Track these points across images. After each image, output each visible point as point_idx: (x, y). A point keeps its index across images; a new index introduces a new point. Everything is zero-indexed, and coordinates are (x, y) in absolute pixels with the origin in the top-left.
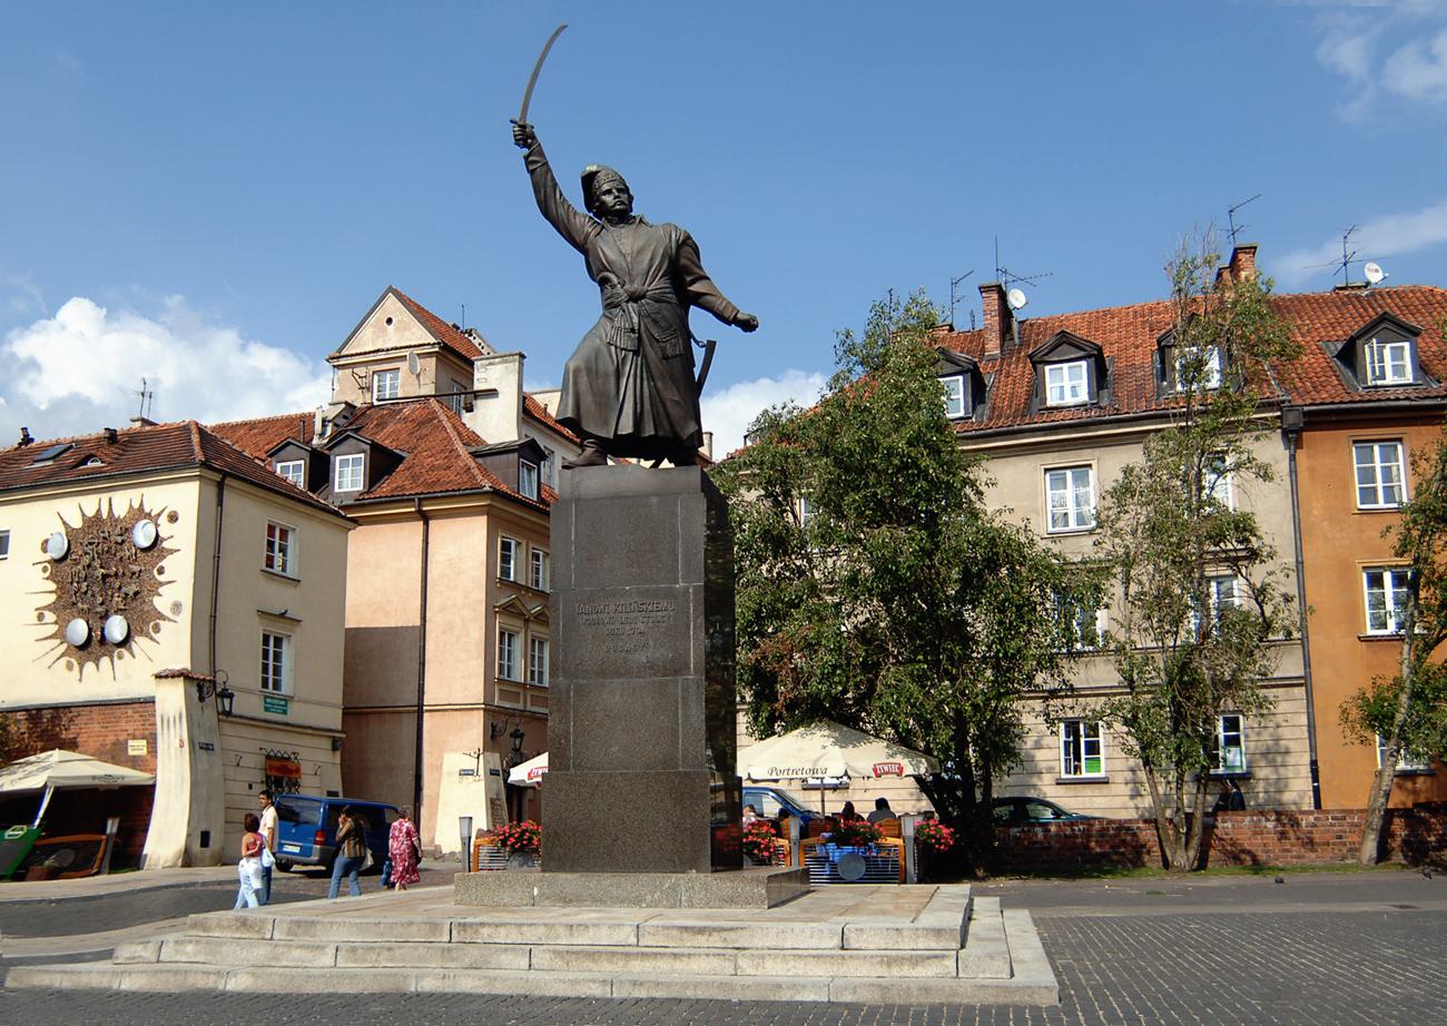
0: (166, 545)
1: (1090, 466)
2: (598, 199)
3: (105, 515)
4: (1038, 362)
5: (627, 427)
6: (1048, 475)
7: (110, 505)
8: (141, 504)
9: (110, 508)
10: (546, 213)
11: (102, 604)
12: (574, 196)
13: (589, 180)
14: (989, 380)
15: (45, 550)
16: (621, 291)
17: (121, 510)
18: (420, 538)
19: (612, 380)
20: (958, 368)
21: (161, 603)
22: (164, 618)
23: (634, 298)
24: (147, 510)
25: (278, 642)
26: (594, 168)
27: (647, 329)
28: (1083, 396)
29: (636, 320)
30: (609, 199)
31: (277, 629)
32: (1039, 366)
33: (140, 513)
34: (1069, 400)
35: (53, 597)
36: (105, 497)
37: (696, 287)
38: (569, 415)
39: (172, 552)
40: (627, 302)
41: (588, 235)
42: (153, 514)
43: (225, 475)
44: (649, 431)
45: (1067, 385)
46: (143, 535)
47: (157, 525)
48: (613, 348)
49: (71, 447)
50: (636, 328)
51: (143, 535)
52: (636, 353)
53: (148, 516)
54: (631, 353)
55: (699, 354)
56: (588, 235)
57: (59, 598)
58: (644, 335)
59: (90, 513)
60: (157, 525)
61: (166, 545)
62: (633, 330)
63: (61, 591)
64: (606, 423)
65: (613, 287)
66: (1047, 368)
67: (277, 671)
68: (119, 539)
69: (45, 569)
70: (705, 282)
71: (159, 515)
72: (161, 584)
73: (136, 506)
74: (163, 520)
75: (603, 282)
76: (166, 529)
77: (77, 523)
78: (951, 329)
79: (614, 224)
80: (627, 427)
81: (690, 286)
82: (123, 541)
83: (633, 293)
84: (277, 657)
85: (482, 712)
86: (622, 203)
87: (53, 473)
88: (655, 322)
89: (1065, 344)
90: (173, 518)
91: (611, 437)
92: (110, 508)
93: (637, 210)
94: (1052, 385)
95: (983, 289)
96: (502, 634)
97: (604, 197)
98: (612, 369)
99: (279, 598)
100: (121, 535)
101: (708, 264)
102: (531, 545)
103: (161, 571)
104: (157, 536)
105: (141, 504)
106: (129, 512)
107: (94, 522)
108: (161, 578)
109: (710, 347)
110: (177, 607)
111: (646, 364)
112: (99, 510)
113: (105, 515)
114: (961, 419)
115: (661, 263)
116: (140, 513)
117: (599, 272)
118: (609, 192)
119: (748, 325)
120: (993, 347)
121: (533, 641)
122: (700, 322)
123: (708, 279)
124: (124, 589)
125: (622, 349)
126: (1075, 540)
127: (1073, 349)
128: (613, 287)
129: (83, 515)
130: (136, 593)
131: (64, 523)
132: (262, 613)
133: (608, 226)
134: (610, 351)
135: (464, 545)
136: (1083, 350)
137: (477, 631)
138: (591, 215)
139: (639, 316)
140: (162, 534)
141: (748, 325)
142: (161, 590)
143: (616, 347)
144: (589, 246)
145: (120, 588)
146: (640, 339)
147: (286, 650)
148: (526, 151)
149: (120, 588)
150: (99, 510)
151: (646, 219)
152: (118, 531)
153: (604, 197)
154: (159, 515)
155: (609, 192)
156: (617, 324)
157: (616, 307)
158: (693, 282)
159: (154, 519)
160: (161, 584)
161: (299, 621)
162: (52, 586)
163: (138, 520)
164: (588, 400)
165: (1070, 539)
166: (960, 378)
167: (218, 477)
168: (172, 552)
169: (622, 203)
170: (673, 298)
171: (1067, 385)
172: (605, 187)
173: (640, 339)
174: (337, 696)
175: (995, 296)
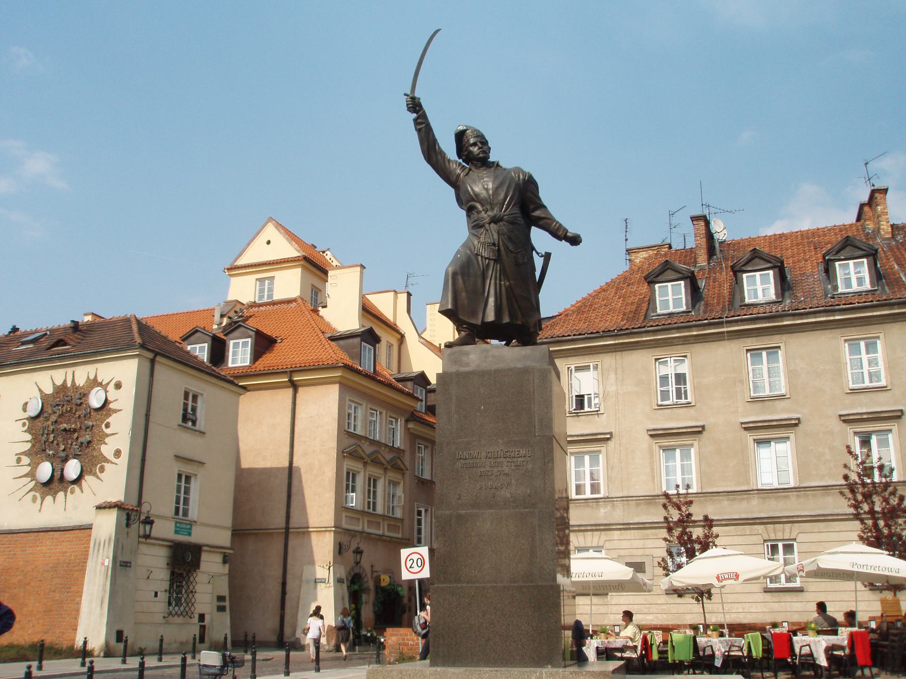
0: (111, 406)
1: (779, 347)
2: (467, 149)
3: (69, 384)
4: (737, 271)
5: (491, 317)
6: (749, 354)
8: (96, 376)
9: (73, 379)
11: (64, 450)
12: (448, 147)
13: (460, 137)
14: (702, 284)
15: (25, 410)
17: (81, 381)
18: (290, 401)
19: (480, 282)
20: (680, 275)
21: (107, 450)
22: (107, 461)
23: (495, 220)
24: (100, 380)
25: (188, 479)
27: (504, 244)
28: (772, 295)
29: (496, 236)
30: (475, 150)
31: (187, 469)
32: (739, 274)
33: (94, 383)
34: (761, 299)
35: (29, 445)
36: (70, 371)
37: (537, 213)
38: (450, 307)
39: (116, 411)
40: (490, 223)
41: (459, 175)
44: (506, 320)
45: (760, 287)
46: (95, 400)
47: (106, 392)
48: (480, 258)
51: (95, 400)
52: (495, 261)
53: (100, 384)
54: (492, 263)
55: (538, 262)
56: (459, 175)
57: (33, 446)
58: (502, 248)
59: (59, 382)
60: (106, 392)
61: (111, 406)
63: (35, 440)
64: (474, 314)
65: (479, 212)
66: (745, 276)
67: (186, 501)
68: (79, 402)
69: (24, 425)
70: (543, 210)
71: (108, 384)
72: (108, 435)
73: (92, 377)
74: (111, 388)
75: (470, 210)
76: (112, 394)
77: (49, 390)
78: (670, 247)
79: (477, 167)
80: (491, 317)
82: (81, 404)
83: (494, 217)
84: (187, 491)
86: (484, 152)
87: (32, 353)
88: (510, 239)
89: (757, 256)
90: (118, 386)
93: (492, 158)
94: (750, 288)
95: (694, 219)
96: (348, 473)
97: (471, 149)
98: (479, 273)
99: (188, 444)
100: (80, 399)
101: (544, 195)
102: (369, 406)
103: (108, 426)
104: (106, 400)
105: (96, 376)
107: (61, 389)
108: (108, 431)
109: (547, 257)
110: (118, 453)
111: (503, 271)
112: (65, 381)
113: (69, 384)
114: (683, 312)
116: (94, 383)
117: (467, 202)
118: (475, 144)
119: (575, 241)
120: (702, 261)
121: (370, 479)
122: (539, 238)
123: (545, 207)
124: (80, 440)
126: (770, 403)
127: (762, 262)
128: (479, 212)
129: (54, 384)
130: (89, 442)
131: (40, 390)
132: (177, 457)
133: (473, 169)
135: (322, 406)
136: (770, 262)
137: (330, 472)
138: (461, 161)
139: (498, 233)
140: (109, 399)
141: (575, 241)
142: (107, 440)
144: (460, 183)
145: (77, 438)
147: (194, 485)
148: (415, 115)
149: (77, 438)
150: (65, 381)
151: (501, 164)
152: (78, 396)
153: (471, 149)
154: (108, 384)
155: (475, 144)
156: (482, 240)
157: (482, 226)
158: (534, 210)
159: (105, 387)
160: (108, 435)
161: (202, 463)
162: (29, 437)
163: (92, 388)
165: (767, 403)
166: (682, 283)
167: (150, 355)
168: (116, 411)
169: (484, 152)
170: (521, 221)
171: (760, 287)
172: (472, 141)
173: (499, 250)
174: (228, 521)
175: (702, 223)
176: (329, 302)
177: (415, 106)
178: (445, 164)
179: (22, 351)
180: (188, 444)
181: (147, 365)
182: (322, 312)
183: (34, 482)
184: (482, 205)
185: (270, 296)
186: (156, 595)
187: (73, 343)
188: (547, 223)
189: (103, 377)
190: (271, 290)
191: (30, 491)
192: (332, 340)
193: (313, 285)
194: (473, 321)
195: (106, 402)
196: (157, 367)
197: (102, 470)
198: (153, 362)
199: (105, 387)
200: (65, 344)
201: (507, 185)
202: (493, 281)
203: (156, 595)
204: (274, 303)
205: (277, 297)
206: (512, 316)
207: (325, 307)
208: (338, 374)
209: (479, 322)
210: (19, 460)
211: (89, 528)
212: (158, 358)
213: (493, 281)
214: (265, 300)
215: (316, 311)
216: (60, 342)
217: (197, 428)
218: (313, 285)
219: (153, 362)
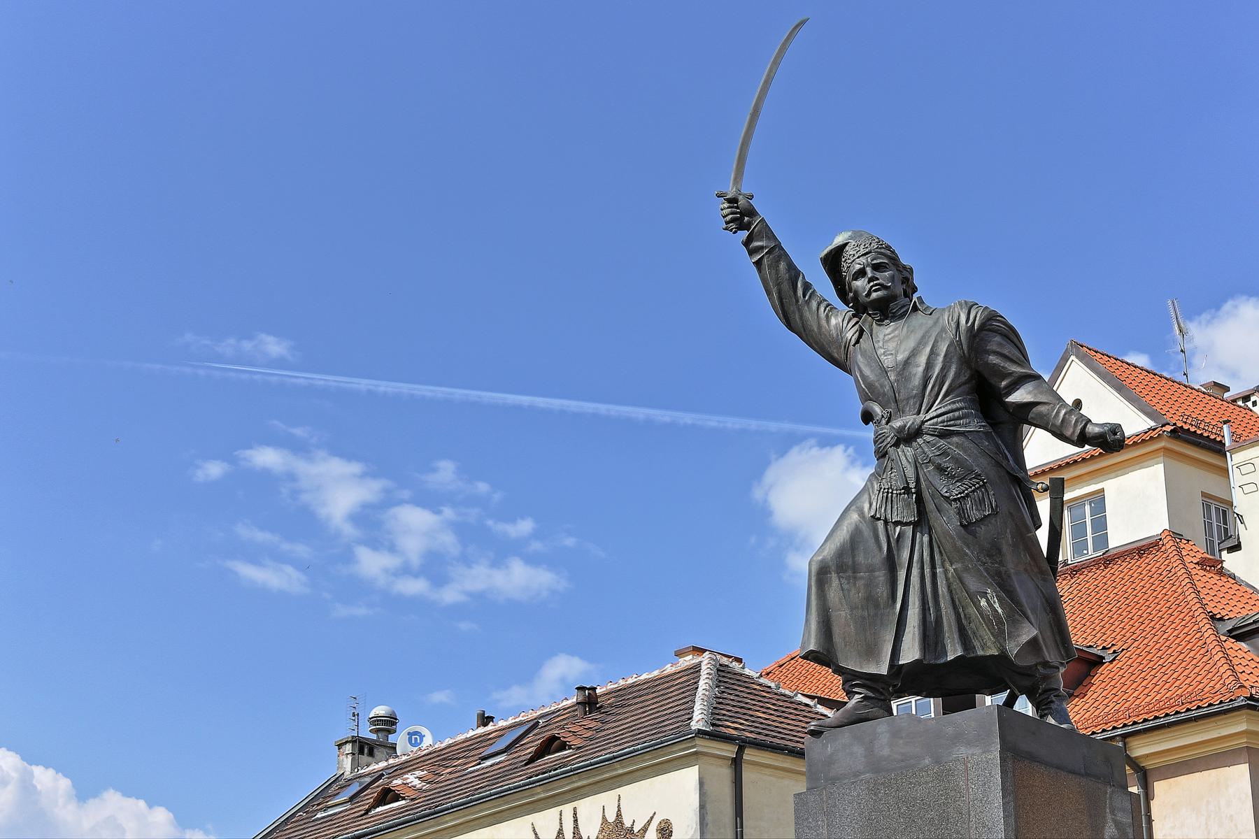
5: (911, 653)
7: (576, 821)
8: (619, 815)
9: (576, 827)
10: (789, 325)
16: (886, 429)
19: (881, 576)
24: (628, 824)
26: (839, 240)
29: (910, 473)
36: (567, 809)
37: (1020, 396)
38: (812, 647)
40: (896, 445)
42: (636, 830)
43: (743, 744)
44: (953, 652)
48: (880, 524)
49: (536, 725)
50: (912, 485)
52: (916, 525)
62: (907, 489)
64: (871, 652)
73: (611, 818)
81: (1009, 394)
83: (901, 429)
87: (504, 774)
88: (941, 470)
91: (884, 670)
98: (878, 558)
105: (619, 815)
106: (602, 830)
115: (945, 369)
125: (897, 523)
134: (875, 531)
143: (886, 522)
146: (920, 501)
148: (744, 234)
155: (861, 273)
164: (842, 616)
167: (730, 751)
173: (920, 501)
176: (1245, 534)
177: (741, 216)
178: (820, 326)
179: (483, 774)
181: (726, 773)
182: (1231, 561)
184: (883, 407)
185: (1102, 540)
187: (577, 742)
188: (1041, 415)
190: (1100, 524)
192: (1239, 638)
193: (1204, 495)
194: (871, 669)
196: (748, 775)
198: (737, 763)
200: (563, 746)
201: (928, 349)
202: (915, 571)
204: (1108, 560)
205: (1118, 538)
207: (1237, 547)
208: (1239, 725)
209: (884, 670)
212: (749, 755)
213: (915, 571)
214: (1091, 553)
215: (1212, 565)
216: (551, 745)
218: (1204, 495)
219: (737, 763)
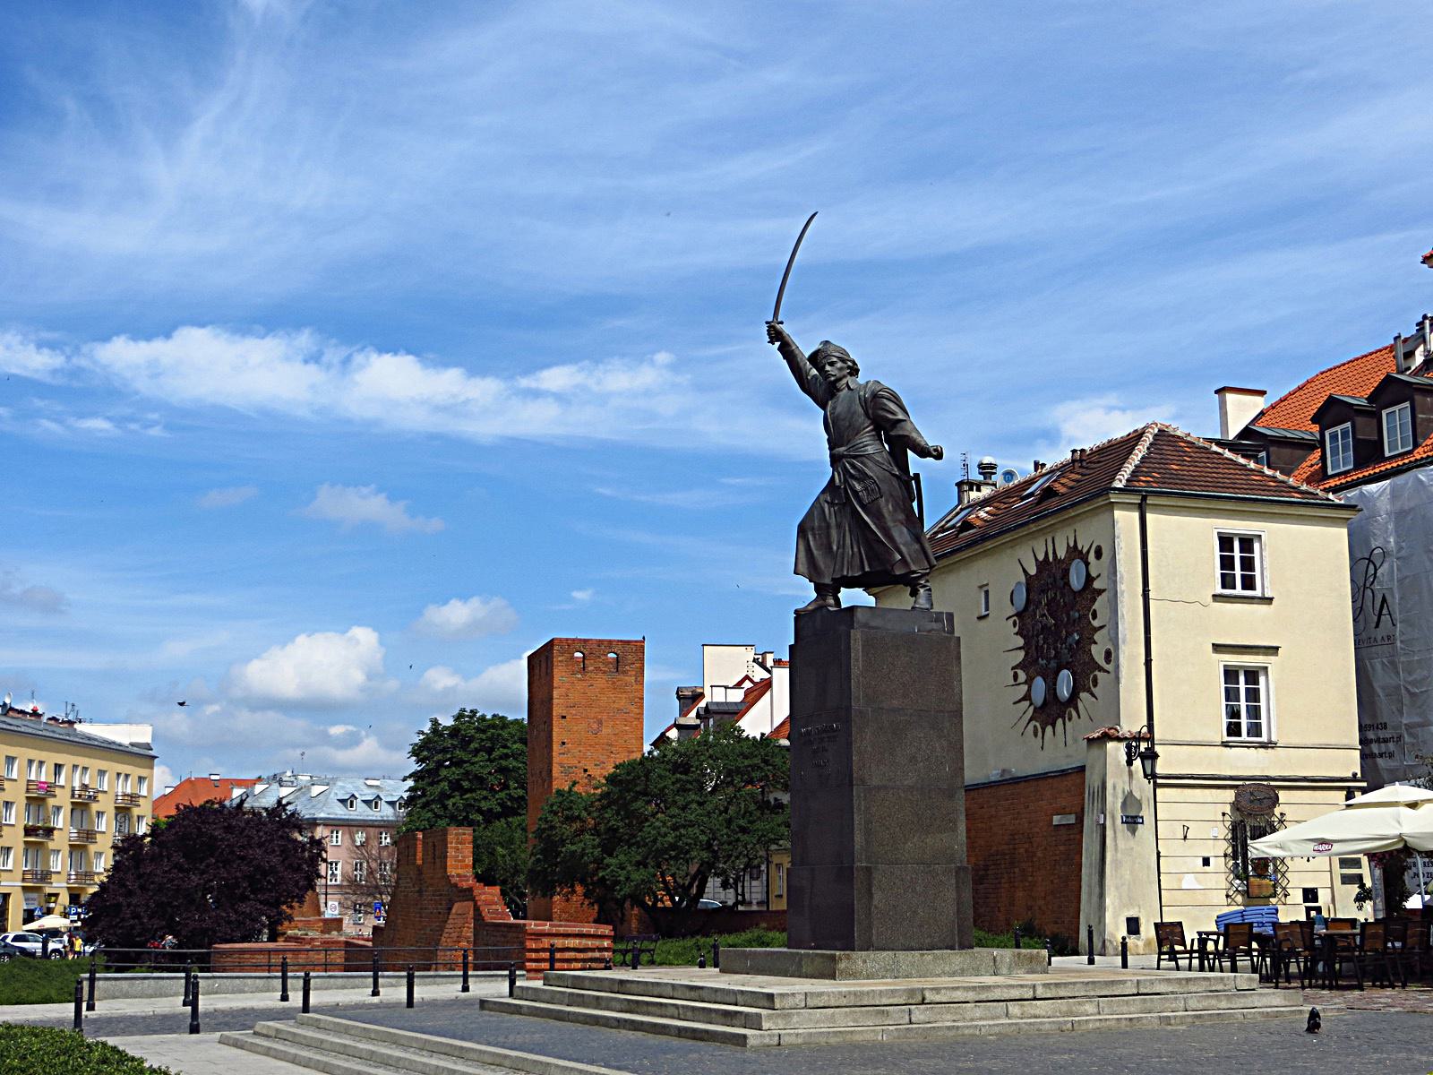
0: (1097, 585)
11: (1055, 657)
25: (1252, 675)
33: (1075, 552)
35: (1021, 654)
39: (1100, 592)
47: (1087, 564)
51: (1076, 582)
61: (1097, 585)
74: (1092, 557)
85: (1359, 752)
92: (1075, 541)
99: (1242, 622)
103: (1095, 617)
108: (1096, 623)
116: (1075, 552)
122: (914, 462)
129: (1036, 560)
130: (1078, 642)
131: (1024, 570)
132: (1217, 648)
140: (1094, 574)
154: (1088, 552)
162: (1020, 642)
168: (1100, 592)
180: (1242, 622)
183: (1032, 708)
186: (1206, 862)
189: (1083, 545)
191: (1030, 720)
195: (1089, 579)
197: (1095, 684)
199: (1084, 558)
203: (1206, 862)
206: (870, 566)
210: (1016, 677)
211: (1082, 769)
217: (1257, 593)
